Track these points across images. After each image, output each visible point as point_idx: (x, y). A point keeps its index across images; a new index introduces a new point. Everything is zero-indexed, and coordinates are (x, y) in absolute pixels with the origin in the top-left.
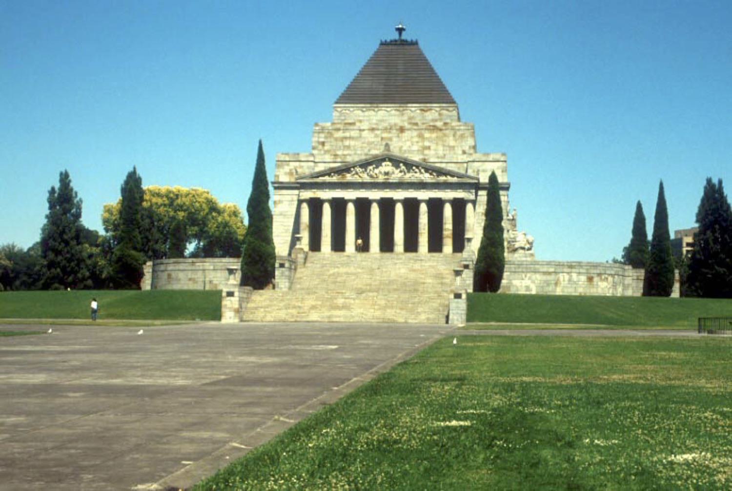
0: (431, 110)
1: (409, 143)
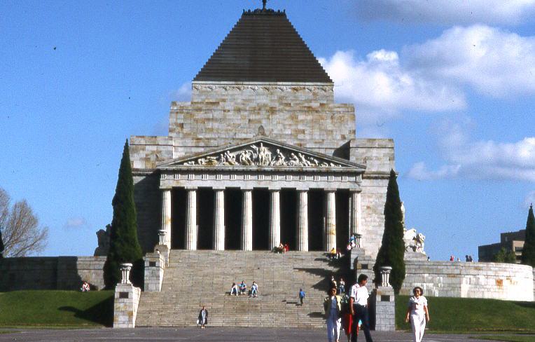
1: (280, 127)
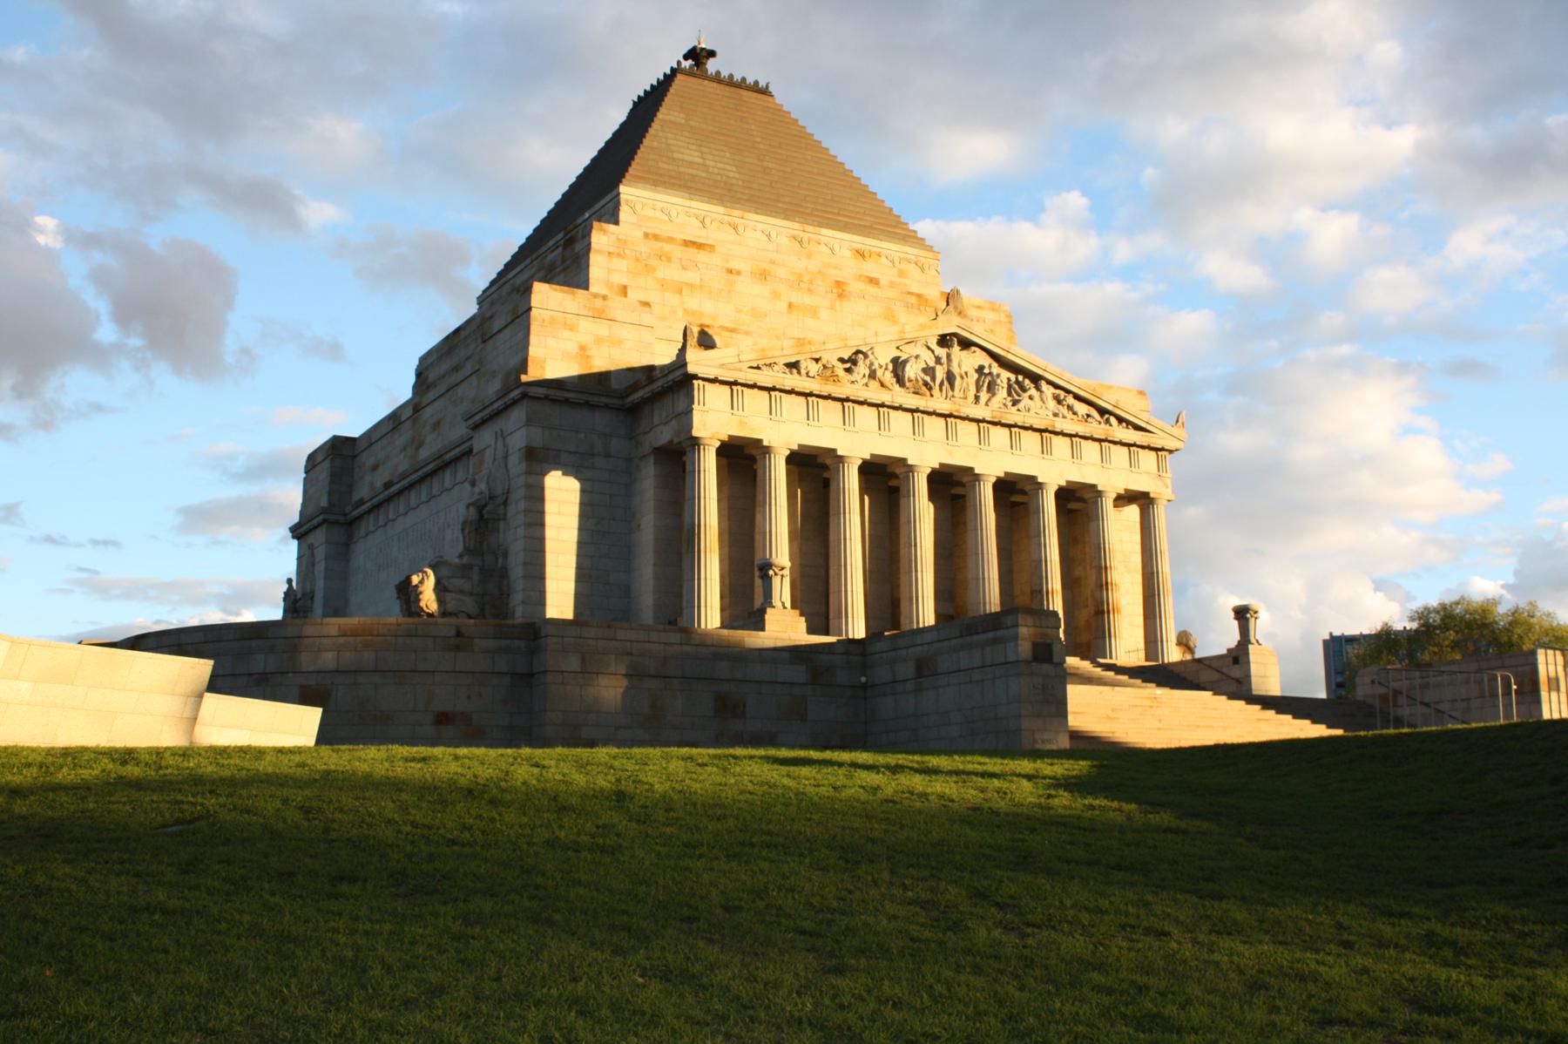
0: (879, 255)
